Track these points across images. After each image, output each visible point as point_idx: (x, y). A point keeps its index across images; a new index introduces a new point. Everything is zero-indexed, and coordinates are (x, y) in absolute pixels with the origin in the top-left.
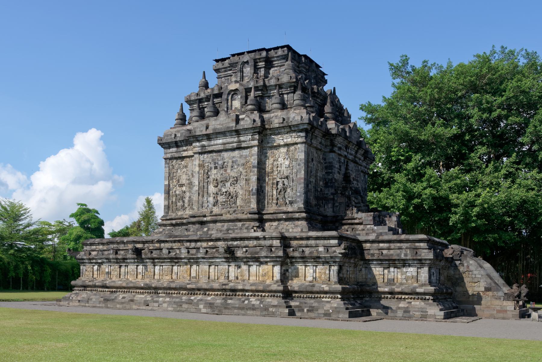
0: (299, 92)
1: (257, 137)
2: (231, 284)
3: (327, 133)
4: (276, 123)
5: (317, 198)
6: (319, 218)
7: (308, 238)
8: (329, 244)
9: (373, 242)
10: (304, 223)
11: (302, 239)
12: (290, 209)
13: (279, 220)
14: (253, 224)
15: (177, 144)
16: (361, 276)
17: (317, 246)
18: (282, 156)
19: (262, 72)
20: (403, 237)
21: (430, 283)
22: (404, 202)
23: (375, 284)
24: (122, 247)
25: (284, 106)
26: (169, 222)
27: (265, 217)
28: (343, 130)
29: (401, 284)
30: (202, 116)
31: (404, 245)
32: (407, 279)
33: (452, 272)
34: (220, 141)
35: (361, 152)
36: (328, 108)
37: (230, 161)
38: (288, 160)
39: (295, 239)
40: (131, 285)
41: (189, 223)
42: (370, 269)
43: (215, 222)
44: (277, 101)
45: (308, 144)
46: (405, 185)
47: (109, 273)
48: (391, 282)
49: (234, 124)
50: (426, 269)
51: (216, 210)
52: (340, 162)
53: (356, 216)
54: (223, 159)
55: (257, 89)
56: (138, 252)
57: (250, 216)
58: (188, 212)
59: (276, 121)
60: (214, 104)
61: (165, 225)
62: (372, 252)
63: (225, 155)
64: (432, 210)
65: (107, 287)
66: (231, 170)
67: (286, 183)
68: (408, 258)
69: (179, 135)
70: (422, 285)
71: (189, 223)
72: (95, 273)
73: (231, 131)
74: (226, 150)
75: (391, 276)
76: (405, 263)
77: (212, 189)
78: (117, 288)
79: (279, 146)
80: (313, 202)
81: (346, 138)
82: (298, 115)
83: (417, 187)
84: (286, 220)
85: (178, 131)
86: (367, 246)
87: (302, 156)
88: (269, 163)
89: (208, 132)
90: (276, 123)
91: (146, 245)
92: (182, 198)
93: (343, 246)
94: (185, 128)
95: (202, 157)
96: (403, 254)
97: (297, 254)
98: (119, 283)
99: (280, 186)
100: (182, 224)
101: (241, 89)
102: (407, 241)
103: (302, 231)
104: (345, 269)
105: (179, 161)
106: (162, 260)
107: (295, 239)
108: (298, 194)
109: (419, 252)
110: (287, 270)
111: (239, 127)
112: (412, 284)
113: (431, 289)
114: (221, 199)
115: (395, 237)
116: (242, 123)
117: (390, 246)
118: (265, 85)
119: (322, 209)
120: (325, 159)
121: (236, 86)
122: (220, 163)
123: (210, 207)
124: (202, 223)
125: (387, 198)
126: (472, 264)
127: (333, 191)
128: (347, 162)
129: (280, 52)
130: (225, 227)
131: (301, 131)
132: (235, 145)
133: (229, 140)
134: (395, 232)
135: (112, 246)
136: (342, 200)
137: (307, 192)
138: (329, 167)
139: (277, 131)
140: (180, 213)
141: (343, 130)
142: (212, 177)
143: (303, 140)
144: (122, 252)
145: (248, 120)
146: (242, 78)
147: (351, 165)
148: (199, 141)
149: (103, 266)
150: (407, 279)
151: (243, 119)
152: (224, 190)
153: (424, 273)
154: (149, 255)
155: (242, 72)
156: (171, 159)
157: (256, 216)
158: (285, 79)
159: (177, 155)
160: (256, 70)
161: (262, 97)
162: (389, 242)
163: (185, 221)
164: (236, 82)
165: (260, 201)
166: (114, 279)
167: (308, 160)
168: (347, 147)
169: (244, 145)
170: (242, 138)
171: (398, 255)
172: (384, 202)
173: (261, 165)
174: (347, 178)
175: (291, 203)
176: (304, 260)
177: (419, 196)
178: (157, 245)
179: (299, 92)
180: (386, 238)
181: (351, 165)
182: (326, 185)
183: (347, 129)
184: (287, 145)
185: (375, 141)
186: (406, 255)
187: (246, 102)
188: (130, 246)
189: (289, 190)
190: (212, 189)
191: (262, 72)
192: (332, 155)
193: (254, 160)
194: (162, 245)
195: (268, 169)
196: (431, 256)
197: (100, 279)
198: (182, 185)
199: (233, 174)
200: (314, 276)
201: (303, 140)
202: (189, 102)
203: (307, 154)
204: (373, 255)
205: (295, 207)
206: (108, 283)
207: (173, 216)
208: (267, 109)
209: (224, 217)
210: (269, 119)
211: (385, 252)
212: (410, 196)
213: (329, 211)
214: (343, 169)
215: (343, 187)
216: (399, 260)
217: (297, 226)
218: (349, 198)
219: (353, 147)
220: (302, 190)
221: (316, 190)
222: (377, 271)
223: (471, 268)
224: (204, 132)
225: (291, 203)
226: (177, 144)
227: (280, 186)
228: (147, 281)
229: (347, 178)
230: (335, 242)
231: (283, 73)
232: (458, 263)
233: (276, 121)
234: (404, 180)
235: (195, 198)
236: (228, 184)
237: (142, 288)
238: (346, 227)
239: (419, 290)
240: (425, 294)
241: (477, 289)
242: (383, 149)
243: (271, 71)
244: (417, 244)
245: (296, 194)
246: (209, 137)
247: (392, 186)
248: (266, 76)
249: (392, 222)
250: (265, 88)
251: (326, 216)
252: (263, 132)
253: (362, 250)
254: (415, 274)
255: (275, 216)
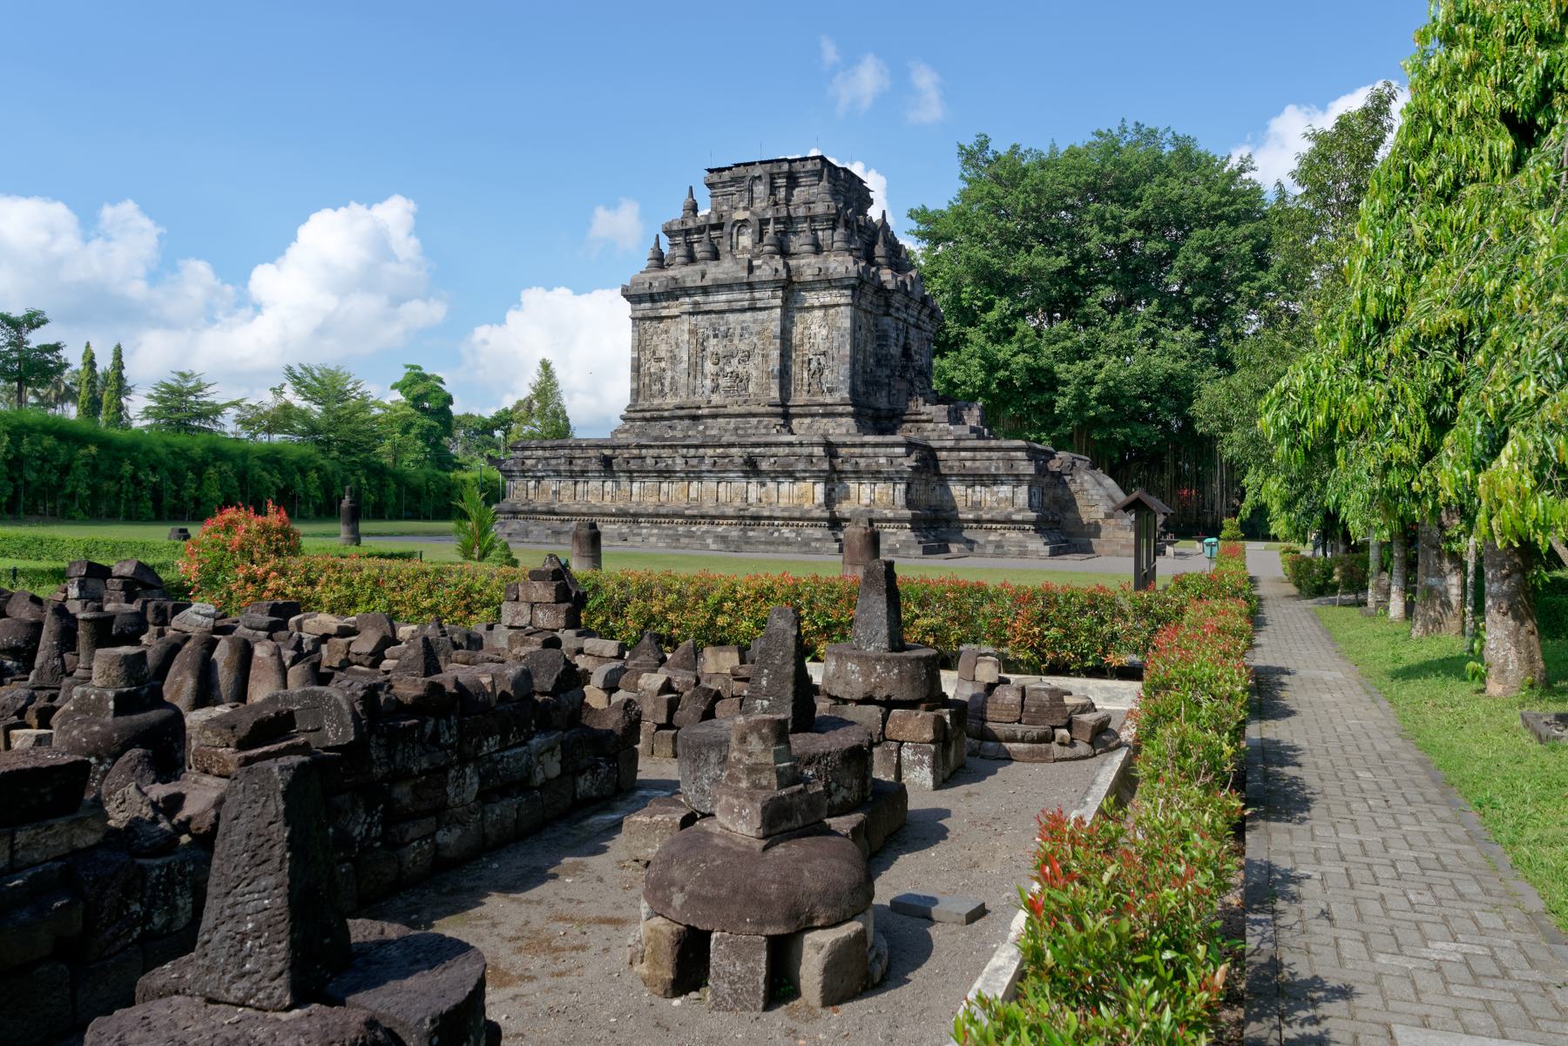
0: (841, 231)
1: (780, 293)
2: (752, 509)
3: (881, 288)
4: (808, 275)
5: (865, 383)
6: (870, 412)
7: (863, 445)
8: (890, 452)
9: (951, 449)
10: (850, 421)
11: (854, 445)
12: (829, 400)
13: (813, 415)
14: (774, 420)
15: (652, 298)
16: (935, 498)
17: (876, 456)
18: (817, 321)
19: (782, 193)
20: (993, 443)
21: (1031, 507)
22: (982, 375)
23: (954, 508)
24: (577, 453)
25: (818, 249)
26: (640, 415)
27: (792, 410)
28: (903, 283)
29: (991, 509)
30: (691, 258)
31: (995, 455)
32: (999, 501)
33: (1060, 492)
35: (926, 311)
36: (880, 250)
38: (826, 328)
39: (845, 445)
40: (595, 510)
41: (674, 418)
42: (948, 487)
43: (715, 416)
44: (809, 240)
45: (856, 306)
46: (983, 348)
47: (555, 492)
48: (977, 506)
49: (745, 274)
50: (1025, 488)
51: (716, 399)
52: (897, 329)
53: (922, 409)
54: (727, 323)
55: (777, 221)
56: (607, 462)
57: (770, 409)
58: (671, 401)
59: (809, 272)
60: (710, 239)
61: (633, 420)
63: (731, 317)
64: (1026, 390)
65: (555, 514)
69: (656, 284)
70: (1020, 510)
71: (674, 418)
72: (531, 492)
73: (741, 284)
74: (732, 311)
75: (977, 498)
76: (995, 480)
77: (709, 367)
78: (572, 514)
79: (813, 308)
80: (861, 389)
81: (907, 294)
82: (841, 264)
83: (1003, 352)
84: (824, 415)
85: (655, 278)
86: (943, 455)
87: (847, 323)
88: (797, 332)
89: (704, 283)
90: (808, 275)
91: (618, 452)
92: (660, 379)
93: (913, 456)
94: (664, 273)
95: (693, 319)
97: (847, 467)
98: (575, 508)
99: (814, 365)
100: (662, 418)
101: (753, 219)
102: (999, 449)
103: (848, 433)
104: (914, 487)
105: (655, 323)
106: (644, 473)
107: (845, 445)
109: (1016, 464)
111: (753, 278)
113: (1032, 515)
115: (981, 443)
116: (757, 272)
118: (789, 216)
119: (872, 399)
120: (876, 325)
121: (747, 215)
123: (705, 393)
124: (695, 418)
125: (955, 369)
127: (888, 372)
129: (809, 166)
130: (732, 426)
131: (845, 288)
132: (746, 304)
133: (737, 296)
134: (981, 437)
135: (561, 452)
136: (903, 386)
137: (852, 377)
138: (882, 337)
139: (810, 286)
140: (656, 402)
141: (903, 283)
142: (710, 349)
143: (849, 300)
144: (580, 462)
145: (768, 268)
146: (751, 200)
147: (913, 331)
148: (689, 295)
149: (545, 482)
150: (999, 501)
151: (759, 267)
152: (729, 370)
153: (1022, 493)
154: (624, 467)
155: (751, 191)
156: (641, 319)
157: (780, 410)
158: (820, 209)
159: (651, 314)
160: (773, 189)
161: (785, 233)
162: (974, 449)
163: (666, 414)
164: (745, 209)
165: (785, 388)
166: (566, 501)
167: (856, 328)
168: (907, 307)
169: (759, 304)
170: (757, 295)
171: (987, 468)
172: (951, 374)
173: (785, 335)
174: (906, 352)
175: (830, 390)
176: (858, 475)
177: (1006, 365)
178: (636, 452)
179: (841, 231)
180: (969, 444)
181: (913, 331)
182: (878, 363)
183: (908, 281)
184: (824, 307)
185: (934, 274)
186: (997, 468)
187: (761, 240)
188: (591, 453)
189: (826, 372)
190: (709, 367)
191: (782, 193)
192: (887, 320)
193: (775, 327)
194: (644, 452)
195: (796, 340)
196: (1032, 470)
197: (540, 502)
198: (659, 360)
199: (743, 346)
201: (849, 300)
202: (669, 233)
203: (854, 320)
204: (951, 468)
205: (837, 397)
206: (556, 506)
207: (646, 405)
208: (792, 250)
209: (729, 410)
210: (798, 267)
211: (968, 464)
212: (991, 366)
213: (882, 402)
214: (902, 340)
215: (903, 367)
217: (840, 425)
218: (911, 383)
220: (847, 373)
221: (865, 372)
222: (957, 490)
223: (1086, 486)
224: (699, 283)
225: (830, 390)
226: (652, 298)
227: (814, 365)
228: (621, 505)
229: (906, 352)
230: (901, 450)
231: (813, 197)
232: (1067, 478)
233: (809, 272)
234: (982, 341)
235: (683, 379)
236: (735, 361)
237: (613, 515)
238: (909, 425)
239: (1015, 517)
240: (1023, 522)
241: (1094, 515)
242: (947, 288)
243: (796, 192)
245: (838, 380)
246: (705, 290)
247: (963, 348)
248: (788, 201)
249: (973, 417)
250: (789, 220)
251: (879, 409)
252: (790, 287)
253: (936, 460)
255: (806, 410)
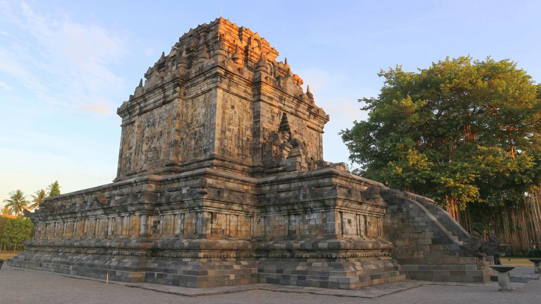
34: (152, 101)
37: (158, 117)
62: (268, 196)
66: (159, 125)
67: (202, 132)
68: (307, 200)
74: (156, 107)
96: (301, 195)
108: (211, 141)
110: (159, 222)
112: (316, 236)
114: (150, 155)
117: (290, 187)
122: (151, 120)
126: (412, 209)
128: (284, 114)
152: (153, 146)
184: (204, 93)
190: (145, 147)
200: (182, 228)
216: (297, 203)
219: (291, 100)
236: (155, 140)
244: (321, 181)
254: (319, 222)
